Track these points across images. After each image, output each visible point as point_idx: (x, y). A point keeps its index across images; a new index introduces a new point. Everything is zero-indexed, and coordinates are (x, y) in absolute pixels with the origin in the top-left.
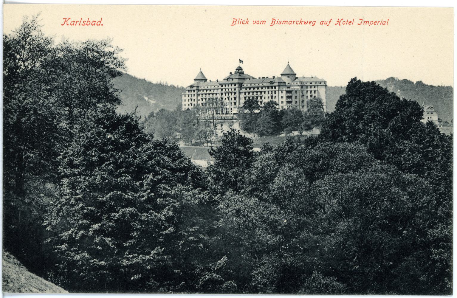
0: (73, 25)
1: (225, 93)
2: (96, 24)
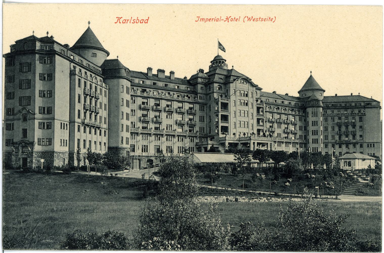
0: (125, 23)
2: (144, 22)
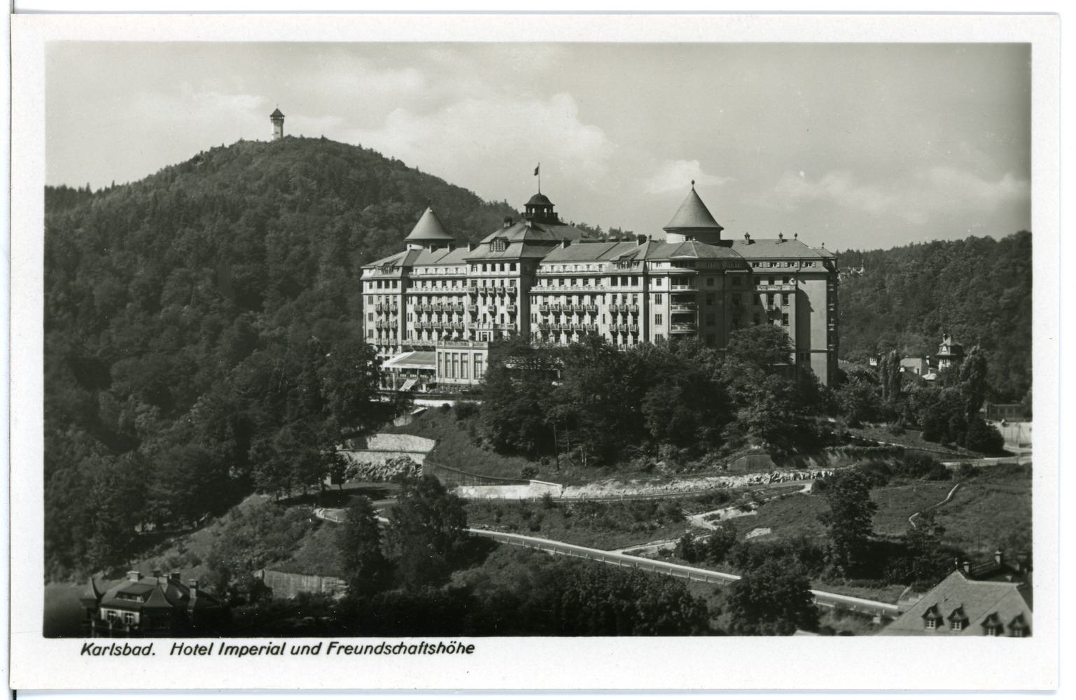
1: (484, 296)
